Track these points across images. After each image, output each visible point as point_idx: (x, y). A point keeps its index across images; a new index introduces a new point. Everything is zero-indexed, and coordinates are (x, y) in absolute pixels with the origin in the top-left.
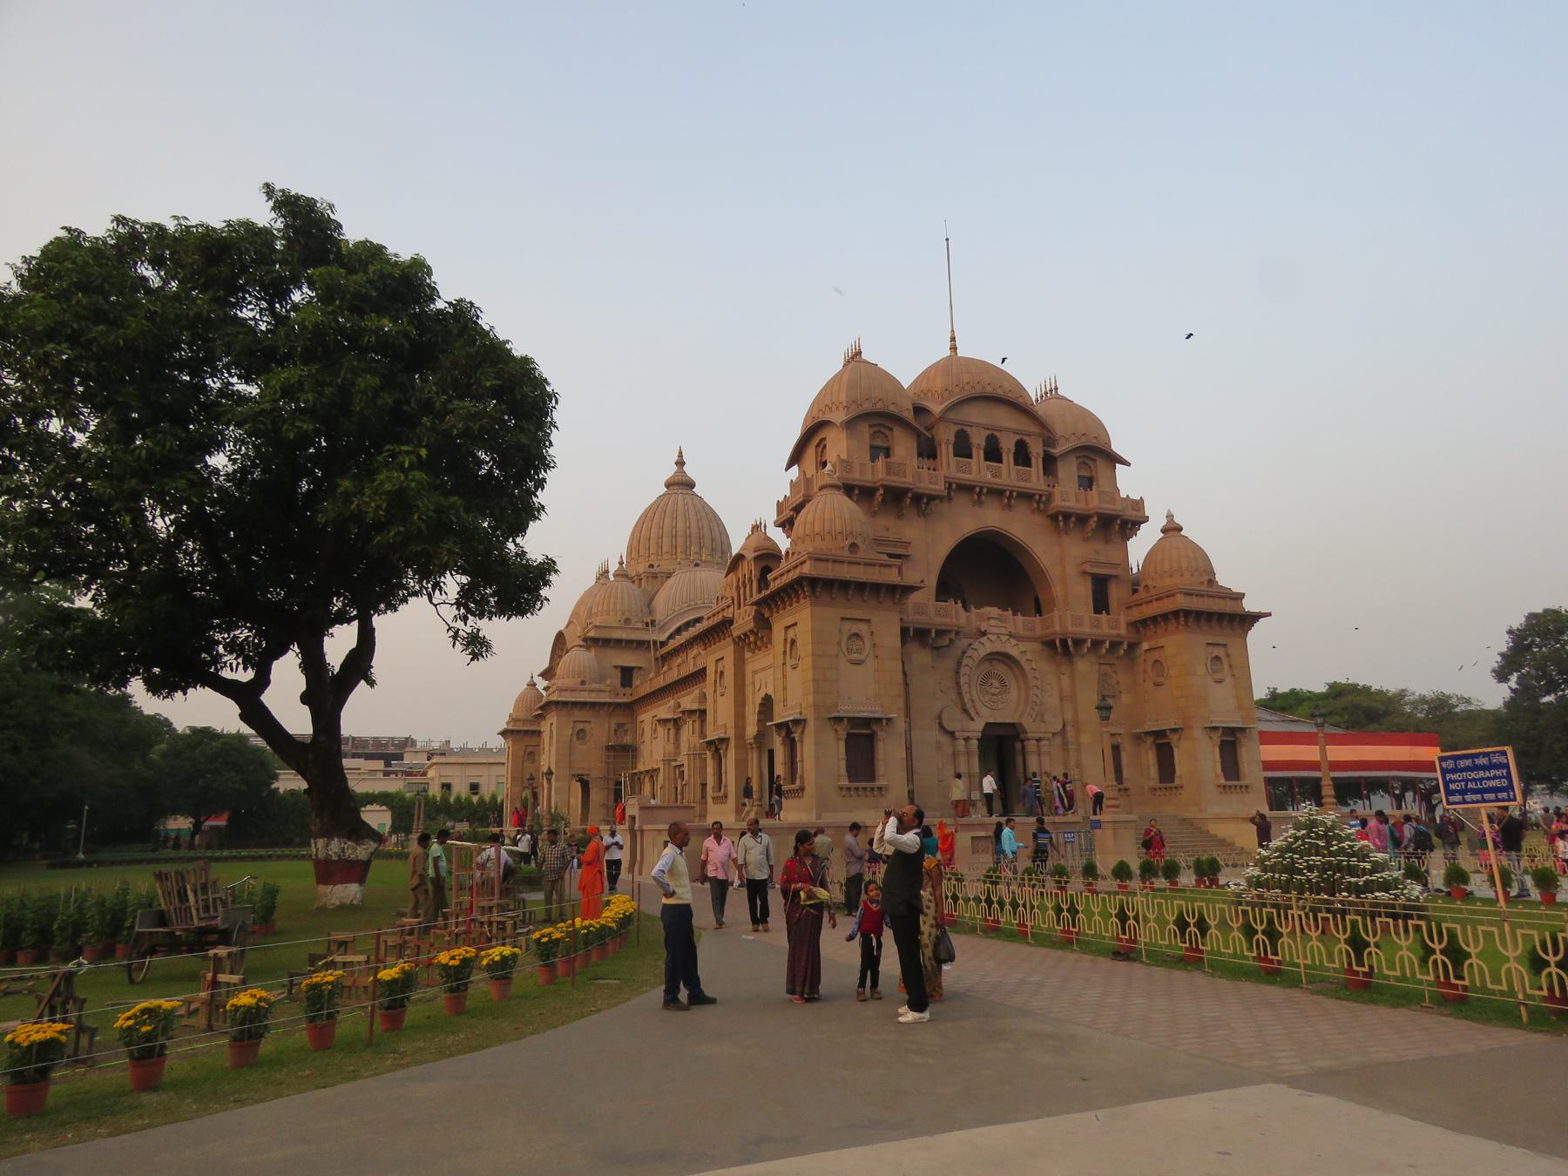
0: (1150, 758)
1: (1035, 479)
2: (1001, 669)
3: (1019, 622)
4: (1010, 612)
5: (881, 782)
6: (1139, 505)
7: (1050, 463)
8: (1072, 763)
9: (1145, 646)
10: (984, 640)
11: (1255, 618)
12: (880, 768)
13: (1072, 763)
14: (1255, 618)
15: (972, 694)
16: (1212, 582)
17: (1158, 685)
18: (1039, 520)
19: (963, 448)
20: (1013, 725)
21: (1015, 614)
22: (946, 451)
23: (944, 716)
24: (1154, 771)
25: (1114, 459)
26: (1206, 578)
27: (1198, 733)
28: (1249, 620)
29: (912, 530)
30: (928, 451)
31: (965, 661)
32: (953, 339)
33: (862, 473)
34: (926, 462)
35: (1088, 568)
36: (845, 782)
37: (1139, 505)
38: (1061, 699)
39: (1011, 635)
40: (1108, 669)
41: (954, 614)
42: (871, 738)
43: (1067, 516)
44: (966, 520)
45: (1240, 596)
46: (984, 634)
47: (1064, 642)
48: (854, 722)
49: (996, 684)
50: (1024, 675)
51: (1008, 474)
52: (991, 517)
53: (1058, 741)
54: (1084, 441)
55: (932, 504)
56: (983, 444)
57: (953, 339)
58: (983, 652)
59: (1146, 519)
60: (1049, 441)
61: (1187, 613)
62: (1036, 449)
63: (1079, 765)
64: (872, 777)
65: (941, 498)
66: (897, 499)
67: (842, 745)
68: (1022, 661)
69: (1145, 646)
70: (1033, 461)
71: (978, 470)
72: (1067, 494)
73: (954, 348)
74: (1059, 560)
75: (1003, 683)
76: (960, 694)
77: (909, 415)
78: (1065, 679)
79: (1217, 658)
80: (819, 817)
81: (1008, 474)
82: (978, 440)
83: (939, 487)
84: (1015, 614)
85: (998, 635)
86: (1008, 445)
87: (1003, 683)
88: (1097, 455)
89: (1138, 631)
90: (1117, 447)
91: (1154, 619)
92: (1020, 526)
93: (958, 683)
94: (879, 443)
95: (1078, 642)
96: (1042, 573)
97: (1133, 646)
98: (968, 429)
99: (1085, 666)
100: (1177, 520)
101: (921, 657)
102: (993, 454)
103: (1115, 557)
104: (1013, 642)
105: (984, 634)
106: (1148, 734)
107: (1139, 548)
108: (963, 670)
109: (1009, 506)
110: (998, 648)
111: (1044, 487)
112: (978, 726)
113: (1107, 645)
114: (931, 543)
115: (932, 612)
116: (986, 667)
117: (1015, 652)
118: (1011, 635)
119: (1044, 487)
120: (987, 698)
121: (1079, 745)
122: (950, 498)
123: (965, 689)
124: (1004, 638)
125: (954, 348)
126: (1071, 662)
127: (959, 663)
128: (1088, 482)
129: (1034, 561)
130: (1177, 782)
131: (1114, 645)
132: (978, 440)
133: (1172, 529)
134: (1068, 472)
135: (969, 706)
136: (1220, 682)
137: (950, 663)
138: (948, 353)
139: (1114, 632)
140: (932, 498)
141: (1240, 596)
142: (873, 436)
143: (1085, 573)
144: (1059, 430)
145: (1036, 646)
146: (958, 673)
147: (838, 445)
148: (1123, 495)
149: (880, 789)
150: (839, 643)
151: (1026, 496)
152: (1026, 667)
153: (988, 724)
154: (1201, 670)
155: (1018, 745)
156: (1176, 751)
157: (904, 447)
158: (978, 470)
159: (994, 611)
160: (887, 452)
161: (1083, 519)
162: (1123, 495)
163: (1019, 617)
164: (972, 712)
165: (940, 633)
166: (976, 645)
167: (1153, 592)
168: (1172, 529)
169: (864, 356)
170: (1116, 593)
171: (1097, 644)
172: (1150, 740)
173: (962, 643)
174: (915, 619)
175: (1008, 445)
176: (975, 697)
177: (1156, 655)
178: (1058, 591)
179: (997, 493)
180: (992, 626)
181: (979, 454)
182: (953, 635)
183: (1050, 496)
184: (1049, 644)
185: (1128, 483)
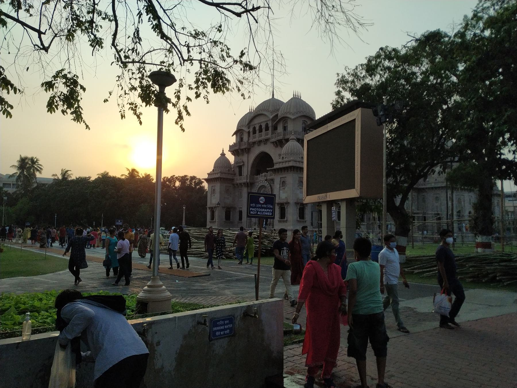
22: (251, 133)
29: (244, 158)
39: (266, 180)
43: (273, 143)
44: (256, 151)
58: (260, 185)
62: (270, 125)
73: (273, 95)
82: (257, 128)
86: (263, 126)
92: (269, 149)
125: (273, 95)
134: (280, 129)
140: (245, 149)
165: (244, 183)
175: (263, 126)
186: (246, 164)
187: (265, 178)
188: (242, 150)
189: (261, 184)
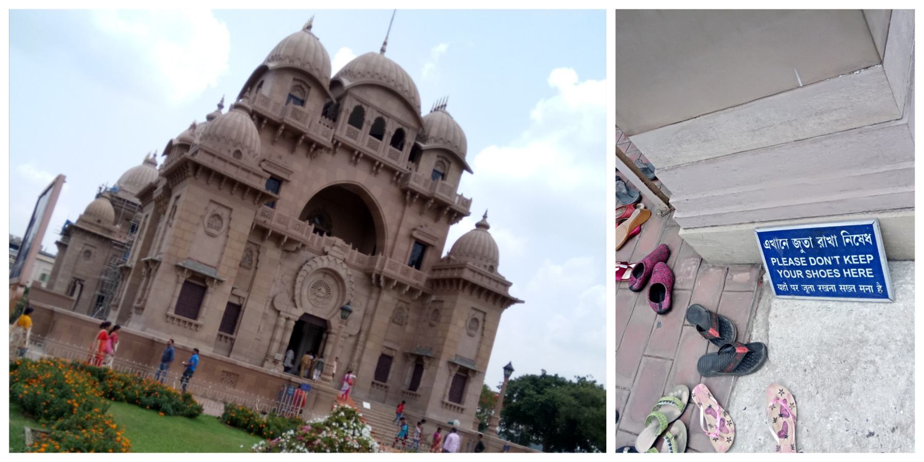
0: (410, 371)
1: (401, 161)
2: (330, 281)
3: (356, 255)
4: (351, 246)
5: (199, 321)
6: (467, 203)
7: (416, 155)
8: (356, 358)
9: (434, 298)
10: (324, 257)
11: (513, 301)
12: (204, 312)
13: (356, 358)
14: (513, 301)
15: (304, 291)
16: (493, 268)
17: (431, 325)
18: (394, 190)
19: (357, 119)
20: (324, 321)
21: (354, 248)
22: (344, 117)
23: (277, 299)
24: (408, 381)
25: (463, 166)
26: (489, 264)
27: (442, 363)
28: (508, 301)
30: (331, 112)
31: (305, 267)
32: (385, 43)
33: (274, 110)
34: (328, 121)
35: (415, 234)
36: (172, 313)
37: (467, 203)
38: (365, 314)
40: (404, 305)
41: (305, 232)
42: (204, 290)
43: (414, 193)
45: (507, 285)
46: (326, 254)
47: (378, 277)
48: (194, 275)
49: (323, 290)
50: (344, 290)
51: (383, 151)
52: (360, 176)
53: (352, 341)
54: (447, 147)
55: (319, 150)
56: (372, 122)
57: (385, 43)
59: (468, 214)
60: (422, 137)
61: (466, 282)
62: (410, 139)
63: (359, 361)
64: (195, 316)
65: (328, 150)
66: (294, 138)
67: (180, 287)
68: (346, 282)
69: (434, 298)
70: (405, 147)
71: (362, 140)
72: (421, 177)
73: (383, 50)
74: (397, 222)
75: (328, 290)
76: (294, 288)
77: (326, 84)
78: (372, 303)
79: (476, 320)
80: (143, 330)
81: (383, 151)
82: (370, 117)
83: (327, 141)
84: (354, 248)
85: (336, 258)
86: (390, 129)
87: (328, 290)
88: (453, 159)
89: (432, 288)
90: (468, 160)
91: (444, 281)
92: (379, 190)
93: (295, 281)
94: (297, 94)
95: (388, 281)
96: (382, 226)
97: (425, 295)
98: (365, 107)
99: (388, 298)
100: (489, 221)
101: (271, 252)
102: (378, 131)
103: (438, 233)
104: (345, 266)
105: (326, 254)
106: (412, 355)
107: (457, 231)
108: (301, 273)
109: (376, 173)
110: (332, 266)
111: (405, 168)
112: (298, 313)
113: (407, 289)
114: (308, 178)
115: (290, 224)
116: (320, 276)
117: (343, 273)
118: (344, 261)
119: (405, 168)
120: (314, 297)
121: (364, 347)
122: (334, 153)
123: (298, 285)
124: (339, 261)
125: (383, 50)
126: (380, 293)
127: (301, 267)
128: (438, 175)
129: (380, 217)
130: (418, 392)
131: (412, 291)
132: (370, 117)
133: (482, 226)
134: (427, 164)
135: (297, 298)
136: (471, 335)
137: (295, 266)
138: (378, 51)
139: (415, 281)
140: (319, 147)
141: (507, 285)
142: (295, 88)
143: (411, 237)
144: (433, 132)
145: (359, 274)
146: (297, 274)
147: (269, 85)
148: (459, 192)
149: (197, 326)
150: (202, 217)
151: (391, 171)
152: (347, 285)
153: (306, 315)
154: (461, 323)
155: (324, 336)
156: (425, 372)
157: (314, 104)
158: (362, 140)
159: (339, 241)
160: (302, 103)
161: (424, 199)
162: (459, 192)
163: (356, 252)
164: (298, 303)
165: (290, 241)
166: (317, 259)
167: (451, 263)
168: (482, 226)
169: (313, 30)
170: (429, 257)
171: (400, 286)
172: (413, 360)
173: (305, 254)
174: (273, 224)
175: (390, 129)
176: (305, 293)
177: (437, 306)
178: (389, 242)
179: (371, 161)
180: (334, 252)
181: (366, 128)
182: (300, 246)
183: (407, 176)
184: (368, 275)
185: (467, 186)
186: (295, 182)
187: (347, 256)
188: (309, 143)
189: (326, 264)
